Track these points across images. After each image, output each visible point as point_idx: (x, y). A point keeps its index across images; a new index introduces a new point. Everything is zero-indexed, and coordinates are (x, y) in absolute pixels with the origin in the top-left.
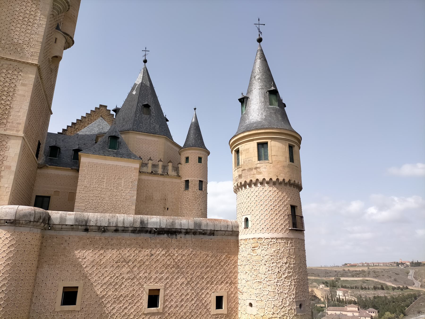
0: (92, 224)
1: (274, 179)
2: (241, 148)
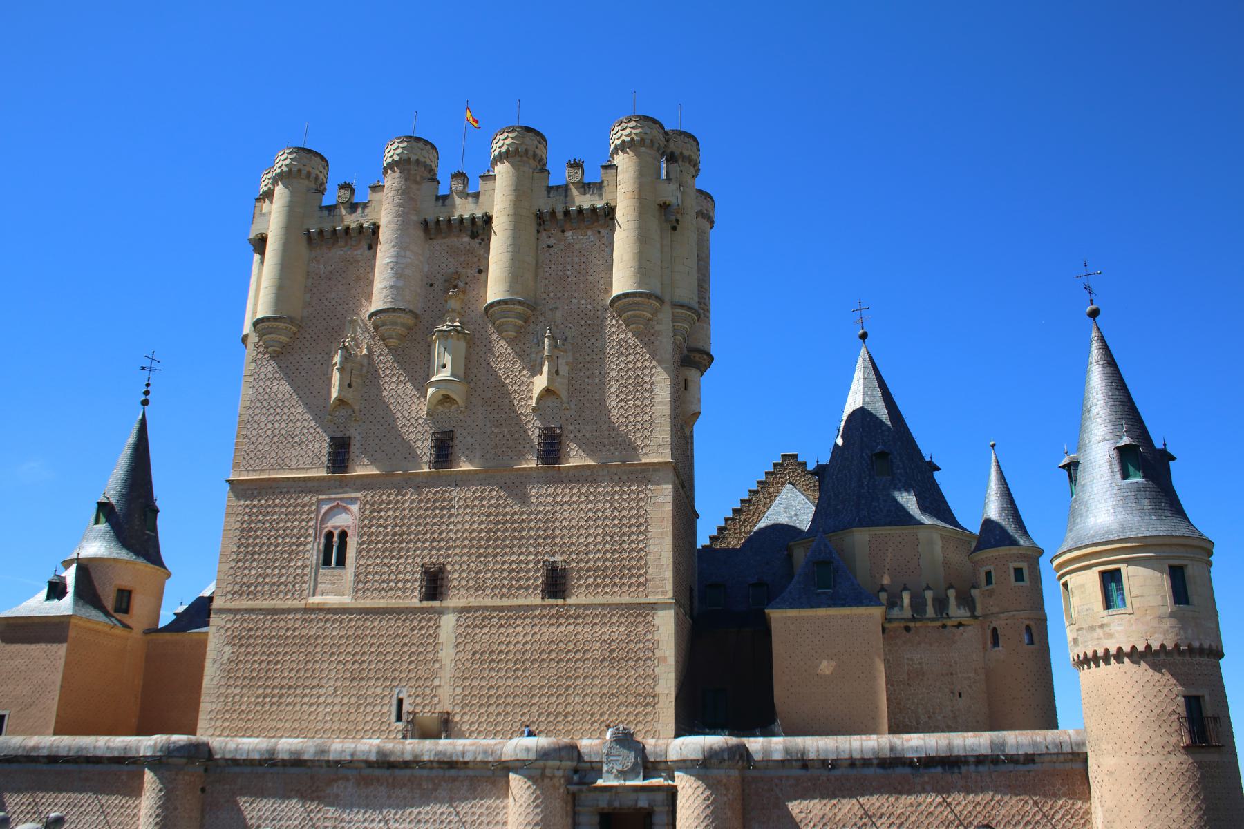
0: (812, 756)
1: (1141, 648)
2: (1072, 580)
